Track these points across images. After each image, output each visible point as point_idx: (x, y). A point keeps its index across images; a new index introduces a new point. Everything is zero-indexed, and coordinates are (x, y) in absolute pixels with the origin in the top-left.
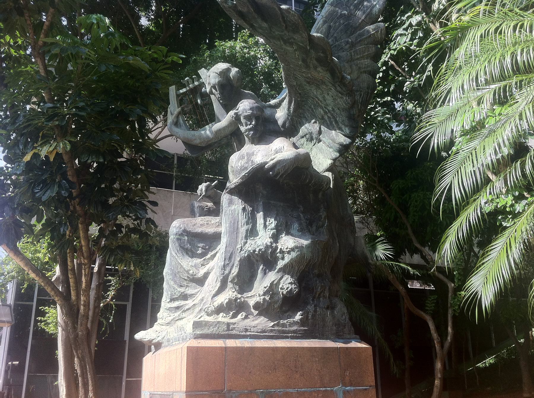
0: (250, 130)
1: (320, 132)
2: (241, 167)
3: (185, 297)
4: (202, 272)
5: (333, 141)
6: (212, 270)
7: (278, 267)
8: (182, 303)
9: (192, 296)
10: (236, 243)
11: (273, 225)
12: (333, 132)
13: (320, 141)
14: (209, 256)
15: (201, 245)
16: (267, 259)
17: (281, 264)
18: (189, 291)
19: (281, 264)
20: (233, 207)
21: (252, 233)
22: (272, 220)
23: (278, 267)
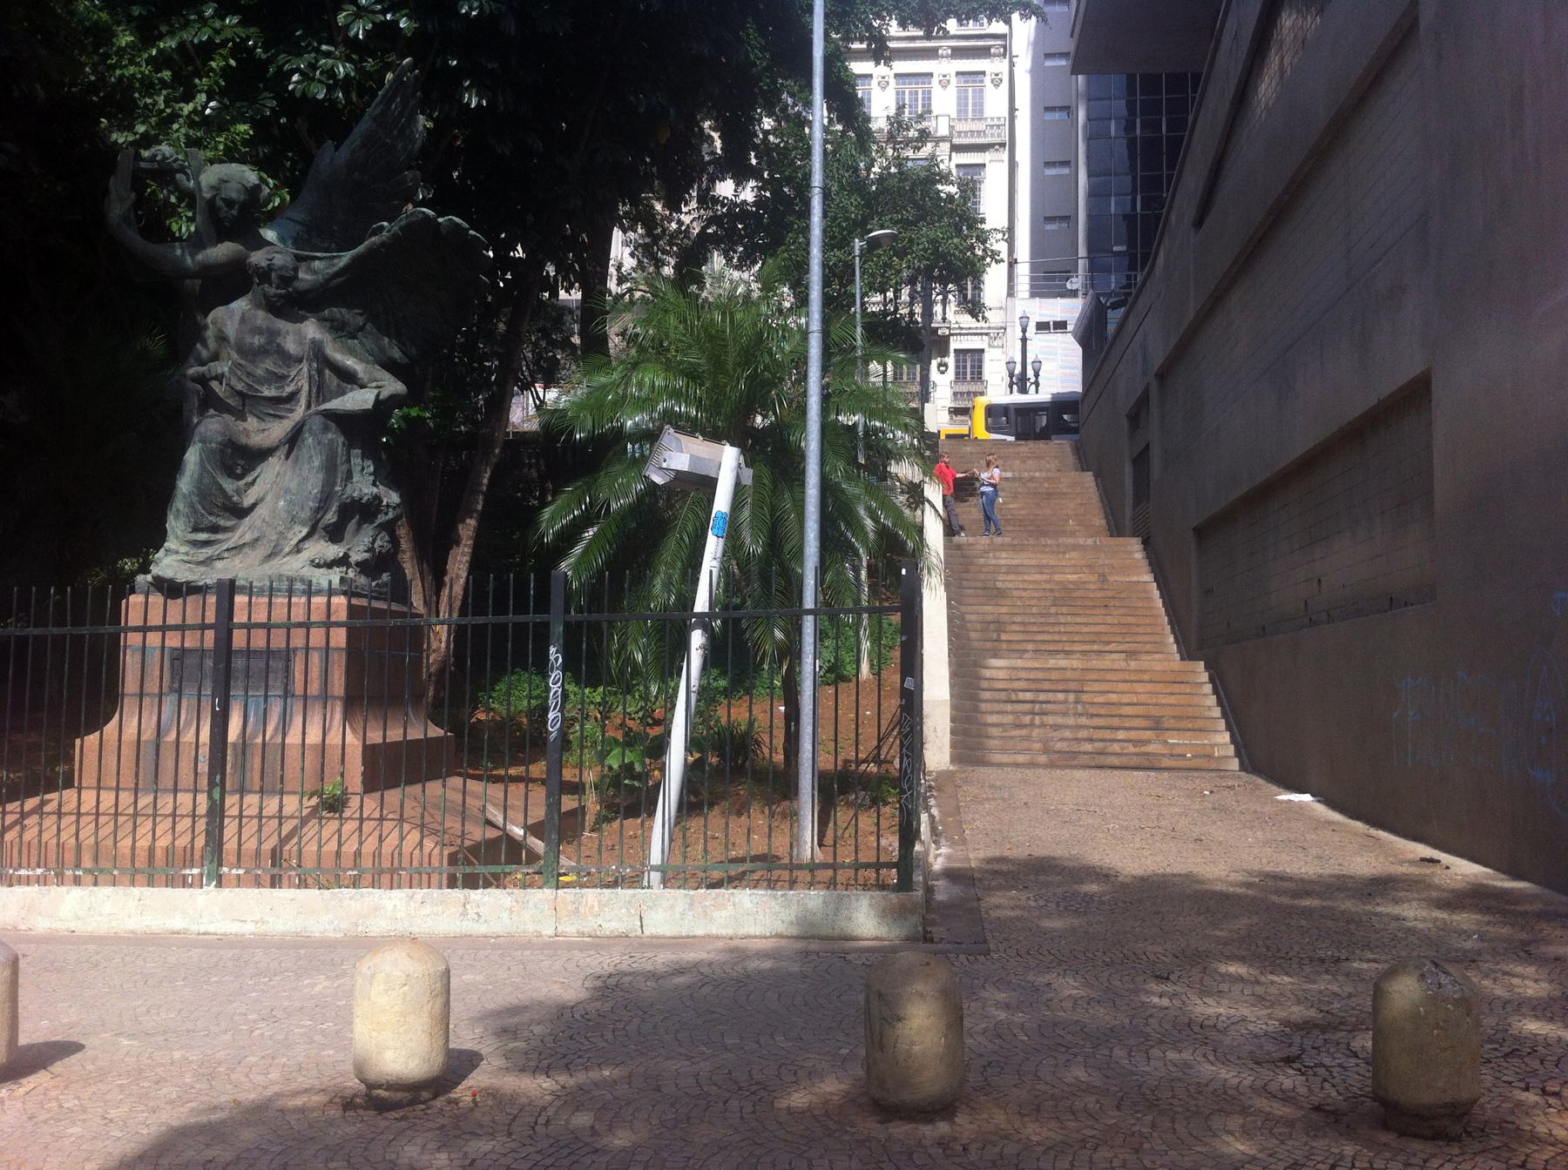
0: (280, 296)
1: (362, 329)
2: (261, 346)
3: (215, 529)
4: (247, 501)
5: (382, 350)
6: (262, 499)
7: (378, 522)
8: (214, 537)
9: (226, 530)
10: (334, 484)
11: (372, 469)
12: (386, 340)
13: (354, 337)
14: (249, 479)
15: (241, 462)
16: (365, 511)
17: (381, 518)
18: (222, 523)
19: (381, 518)
20: (330, 436)
21: (349, 476)
22: (370, 462)
23: (378, 522)
